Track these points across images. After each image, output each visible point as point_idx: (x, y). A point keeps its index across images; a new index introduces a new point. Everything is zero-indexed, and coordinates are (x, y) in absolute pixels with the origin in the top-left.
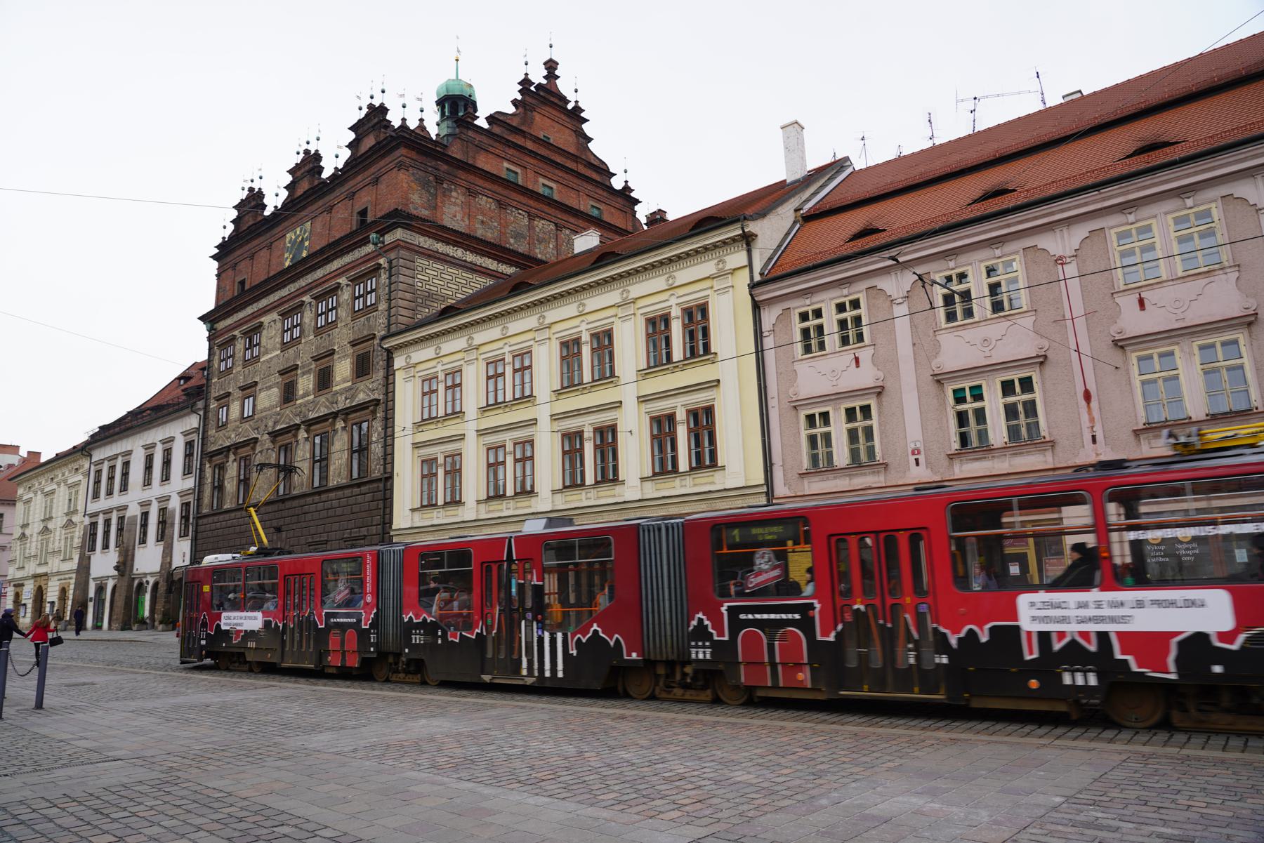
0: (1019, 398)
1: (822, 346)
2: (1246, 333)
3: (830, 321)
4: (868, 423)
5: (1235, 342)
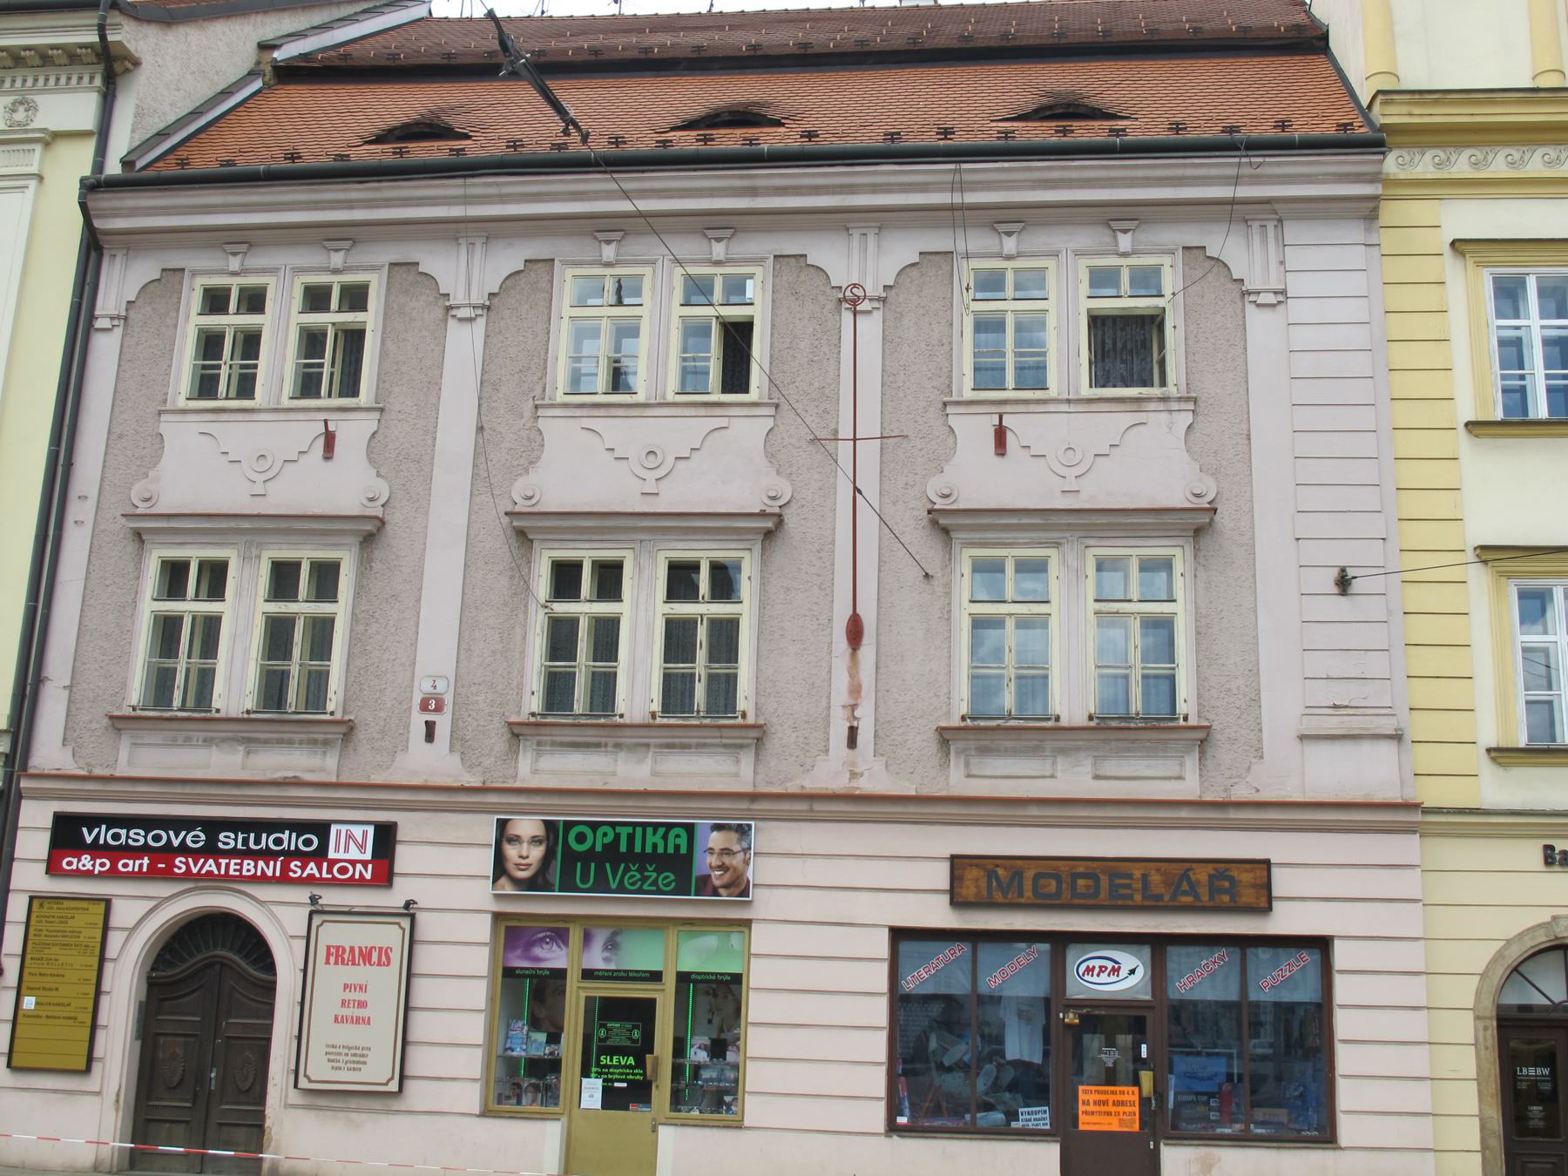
0: (704, 609)
1: (246, 386)
2: (1189, 549)
3: (281, 327)
4: (324, 608)
5: (1166, 565)
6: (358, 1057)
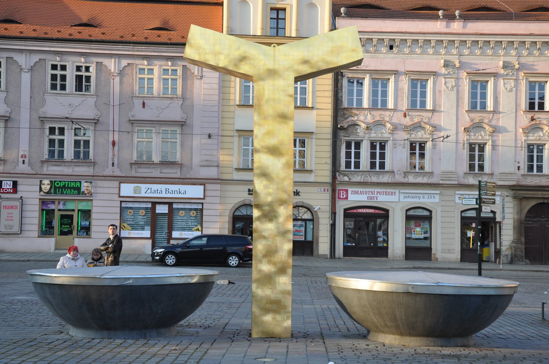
2: (180, 129)
6: (11, 227)
